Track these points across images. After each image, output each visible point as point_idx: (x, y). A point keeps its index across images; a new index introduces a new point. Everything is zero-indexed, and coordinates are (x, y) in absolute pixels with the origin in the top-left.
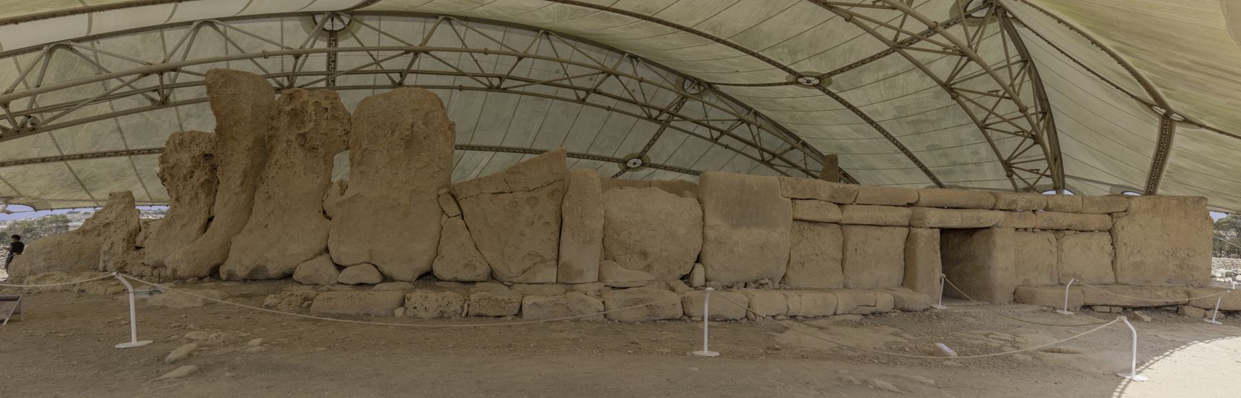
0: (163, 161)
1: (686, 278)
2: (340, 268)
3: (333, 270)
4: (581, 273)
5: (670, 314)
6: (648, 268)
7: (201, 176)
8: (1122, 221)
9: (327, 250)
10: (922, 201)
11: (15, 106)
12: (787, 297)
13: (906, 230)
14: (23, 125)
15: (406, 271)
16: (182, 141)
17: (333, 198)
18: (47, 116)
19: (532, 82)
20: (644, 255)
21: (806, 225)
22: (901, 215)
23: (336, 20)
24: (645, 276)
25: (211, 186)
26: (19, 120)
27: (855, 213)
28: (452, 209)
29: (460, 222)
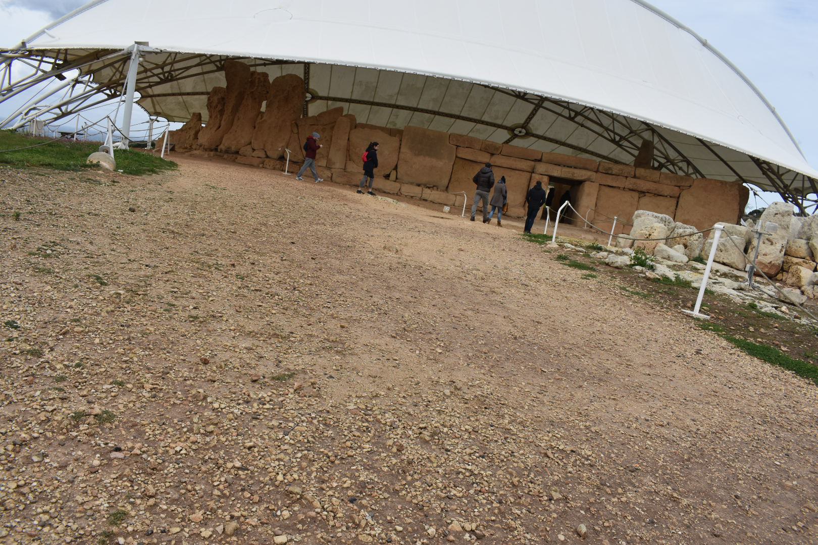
0: (209, 99)
2: (254, 150)
4: (334, 163)
7: (220, 107)
8: (684, 193)
9: (250, 143)
10: (544, 159)
13: (528, 175)
16: (216, 90)
17: (259, 120)
18: (177, 73)
22: (525, 165)
25: (222, 112)
28: (295, 131)
29: (296, 136)
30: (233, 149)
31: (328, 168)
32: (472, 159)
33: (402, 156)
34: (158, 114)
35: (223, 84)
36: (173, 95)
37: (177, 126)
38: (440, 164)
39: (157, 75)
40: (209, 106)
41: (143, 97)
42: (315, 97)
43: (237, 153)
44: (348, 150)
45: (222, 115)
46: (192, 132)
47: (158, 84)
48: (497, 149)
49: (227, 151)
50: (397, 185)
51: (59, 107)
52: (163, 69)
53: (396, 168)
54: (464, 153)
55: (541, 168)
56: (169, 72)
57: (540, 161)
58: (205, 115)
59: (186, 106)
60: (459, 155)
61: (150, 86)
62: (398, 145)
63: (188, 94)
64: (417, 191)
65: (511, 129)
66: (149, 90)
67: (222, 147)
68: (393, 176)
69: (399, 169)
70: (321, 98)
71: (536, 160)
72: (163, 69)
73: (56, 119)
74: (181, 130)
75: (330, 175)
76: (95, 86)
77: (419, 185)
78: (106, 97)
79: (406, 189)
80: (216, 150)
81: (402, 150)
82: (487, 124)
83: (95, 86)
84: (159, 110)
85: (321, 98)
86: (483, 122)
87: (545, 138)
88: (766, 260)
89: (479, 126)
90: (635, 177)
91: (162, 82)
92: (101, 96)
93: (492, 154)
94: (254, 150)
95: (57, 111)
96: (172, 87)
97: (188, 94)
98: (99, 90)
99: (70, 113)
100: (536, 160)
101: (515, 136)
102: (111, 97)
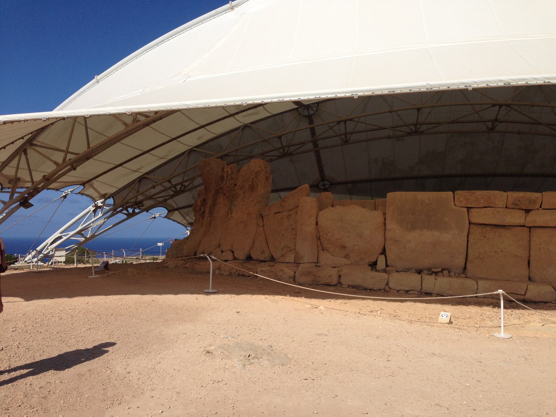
1: (373, 265)
3: (220, 253)
5: (328, 281)
6: (347, 256)
11: (174, 182)
12: (436, 279)
14: (180, 189)
15: (241, 254)
19: (439, 124)
20: (343, 247)
21: (488, 228)
23: (310, 110)
24: (345, 261)
26: (178, 187)
27: (538, 218)
29: (262, 229)
32: (495, 222)
33: (389, 234)
38: (446, 237)
39: (170, 188)
41: (169, 211)
44: (319, 238)
45: (203, 218)
47: (172, 197)
48: (533, 202)
50: (385, 275)
52: (170, 181)
53: (384, 252)
56: (181, 184)
60: (474, 220)
62: (381, 220)
64: (413, 280)
68: (381, 264)
69: (388, 253)
72: (170, 181)
75: (292, 274)
77: (419, 272)
78: (125, 217)
79: (396, 280)
81: (388, 227)
85: (340, 183)
91: (177, 193)
92: (121, 216)
93: (527, 211)
94: (222, 252)
102: (130, 216)
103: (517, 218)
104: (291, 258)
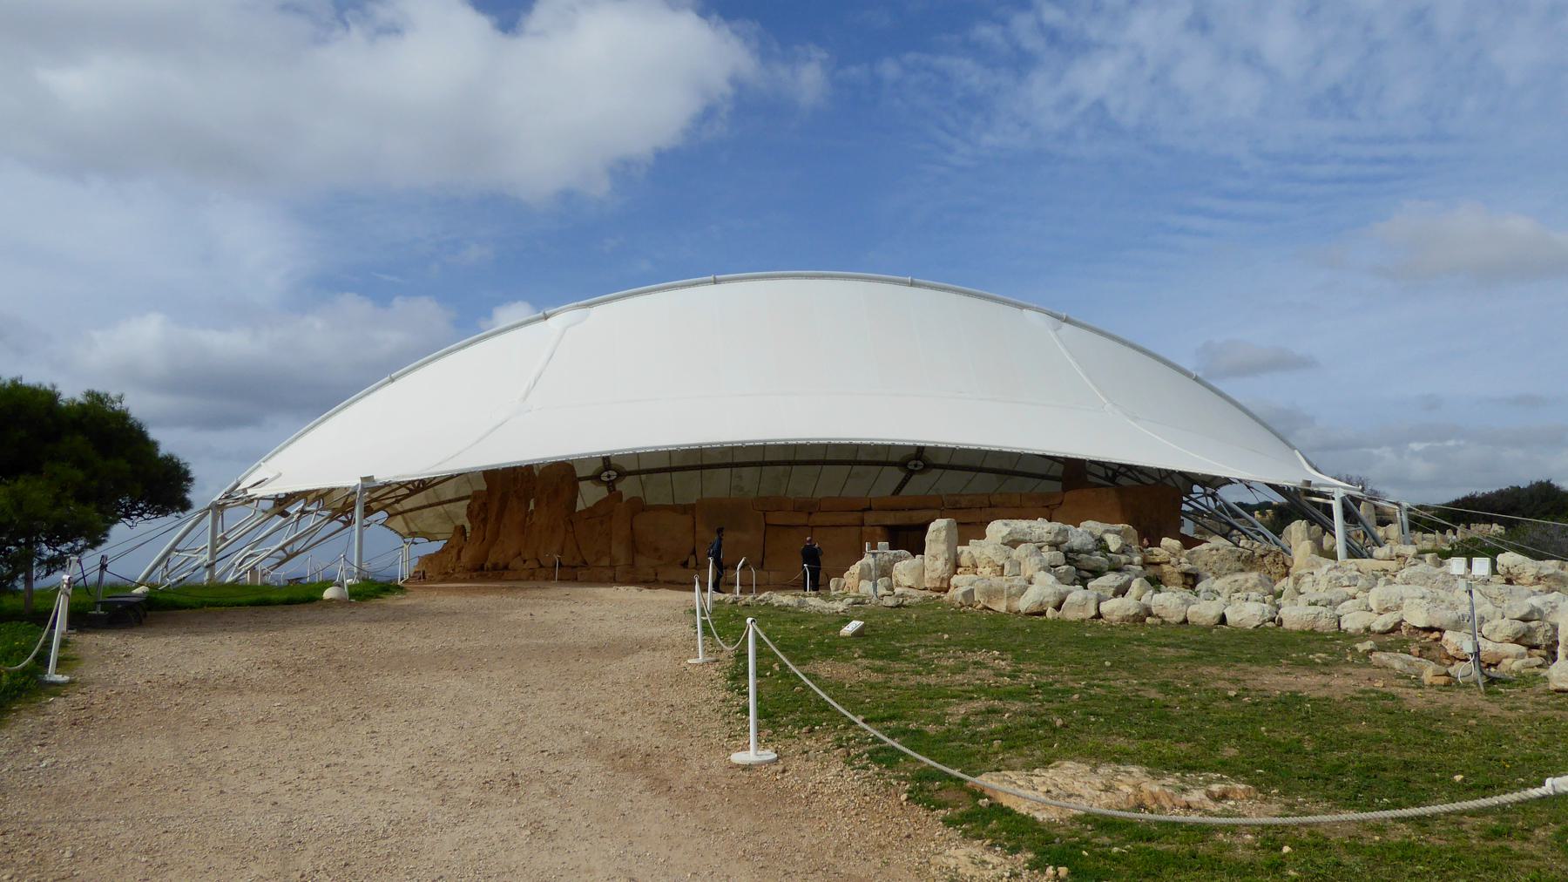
6: (660, 558)
16: (475, 496)
20: (656, 550)
22: (852, 518)
25: (485, 521)
30: (501, 565)
31: (612, 567)
34: (413, 534)
35: (485, 488)
36: (431, 506)
37: (437, 546)
40: (470, 515)
42: (622, 474)
43: (506, 567)
46: (454, 552)
47: (406, 496)
49: (495, 567)
51: (282, 548)
53: (694, 553)
54: (777, 518)
55: (870, 518)
57: (870, 509)
58: (468, 526)
59: (449, 517)
61: (398, 501)
63: (450, 501)
65: (902, 465)
66: (397, 506)
67: (488, 564)
68: (692, 562)
70: (630, 473)
71: (864, 510)
73: (279, 564)
74: (442, 551)
76: (327, 513)
80: (482, 568)
82: (867, 463)
83: (327, 513)
84: (415, 529)
85: (630, 473)
86: (860, 463)
87: (953, 468)
88: (935, 575)
89: (857, 468)
90: (990, 506)
92: (337, 525)
95: (281, 553)
96: (427, 497)
97: (450, 501)
98: (332, 518)
99: (297, 553)
100: (864, 510)
101: (911, 473)
103: (801, 519)
104: (605, 562)
